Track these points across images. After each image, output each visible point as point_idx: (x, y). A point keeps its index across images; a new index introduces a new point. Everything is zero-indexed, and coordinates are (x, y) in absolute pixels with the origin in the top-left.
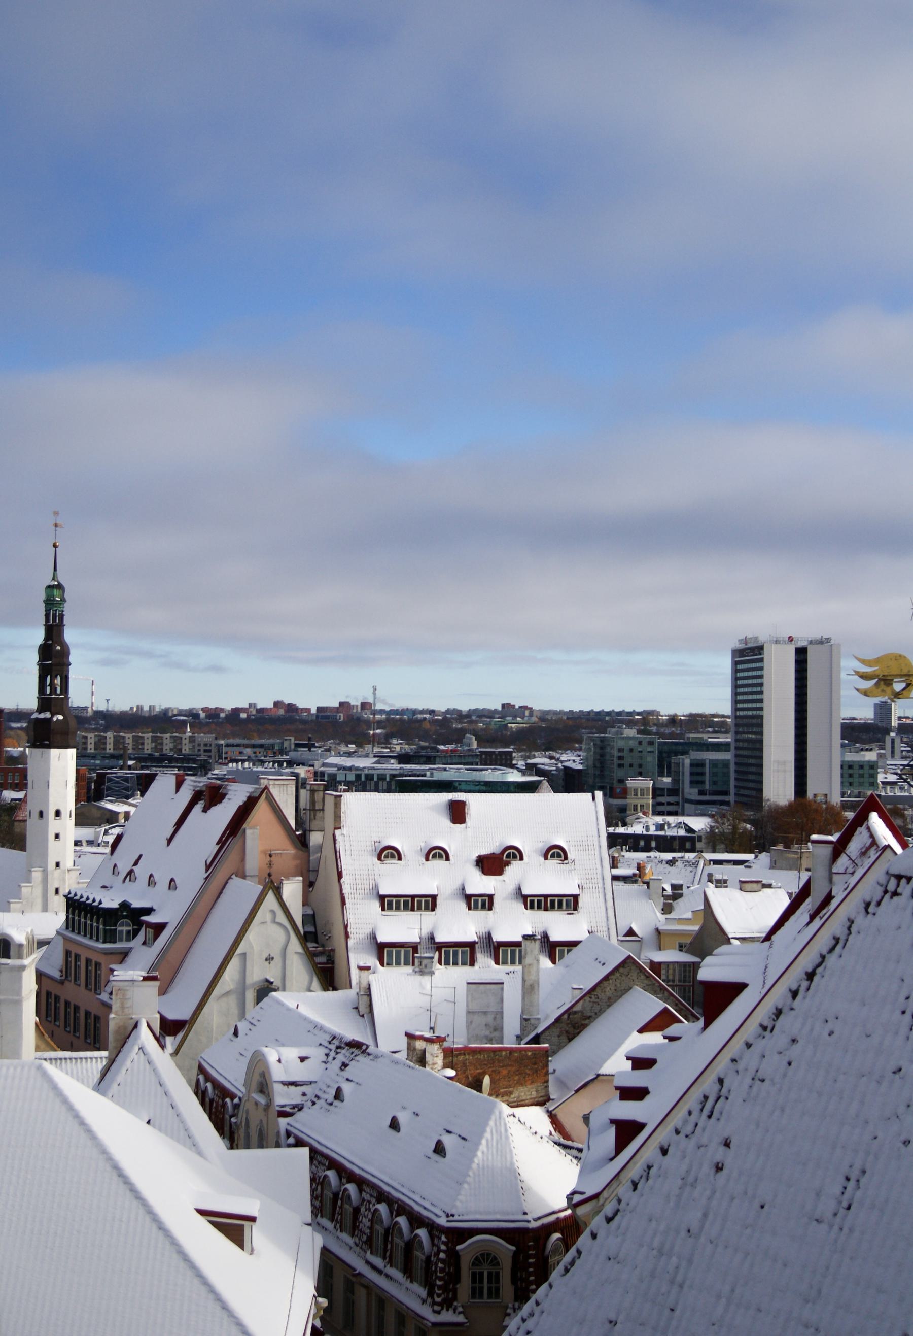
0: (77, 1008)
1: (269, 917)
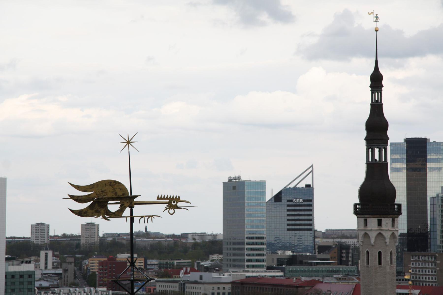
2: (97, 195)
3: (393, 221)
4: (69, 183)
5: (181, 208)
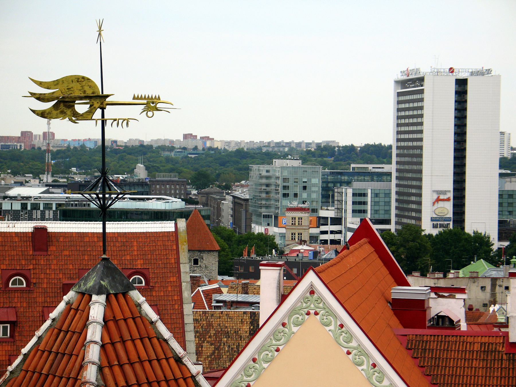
2: (62, 93)
4: (29, 78)
5: (162, 110)
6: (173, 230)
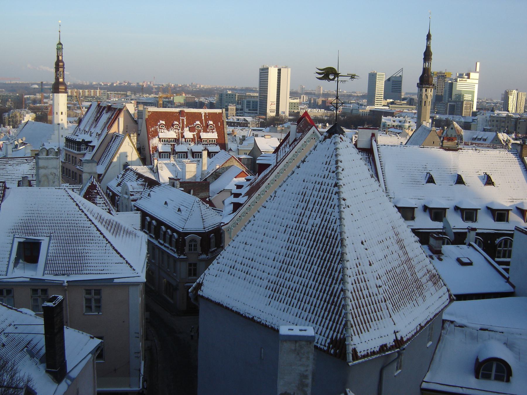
0: (70, 170)
1: (127, 144)
3: (431, 90)
6: (221, 112)
